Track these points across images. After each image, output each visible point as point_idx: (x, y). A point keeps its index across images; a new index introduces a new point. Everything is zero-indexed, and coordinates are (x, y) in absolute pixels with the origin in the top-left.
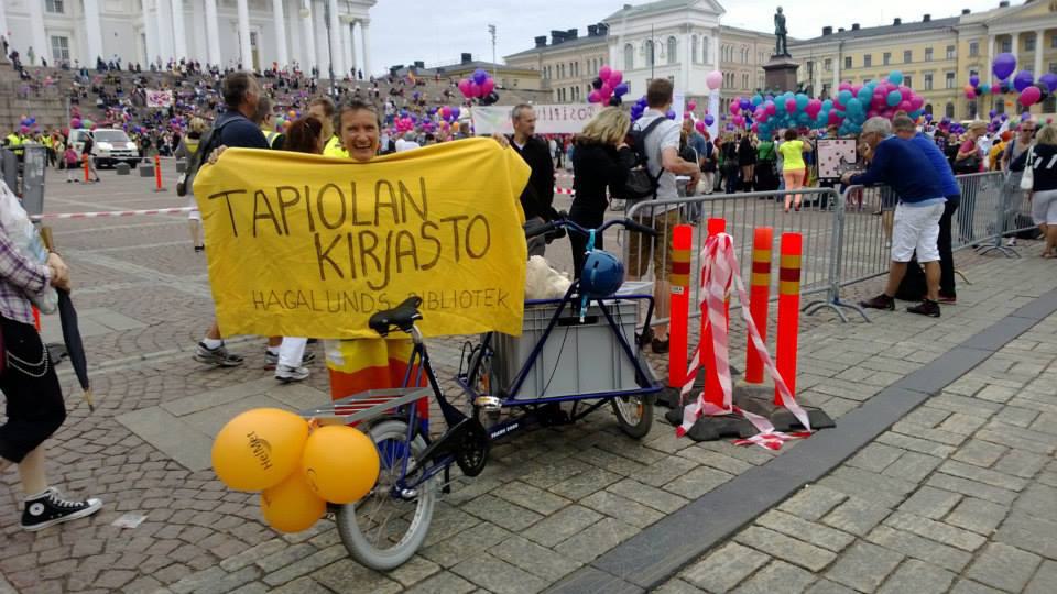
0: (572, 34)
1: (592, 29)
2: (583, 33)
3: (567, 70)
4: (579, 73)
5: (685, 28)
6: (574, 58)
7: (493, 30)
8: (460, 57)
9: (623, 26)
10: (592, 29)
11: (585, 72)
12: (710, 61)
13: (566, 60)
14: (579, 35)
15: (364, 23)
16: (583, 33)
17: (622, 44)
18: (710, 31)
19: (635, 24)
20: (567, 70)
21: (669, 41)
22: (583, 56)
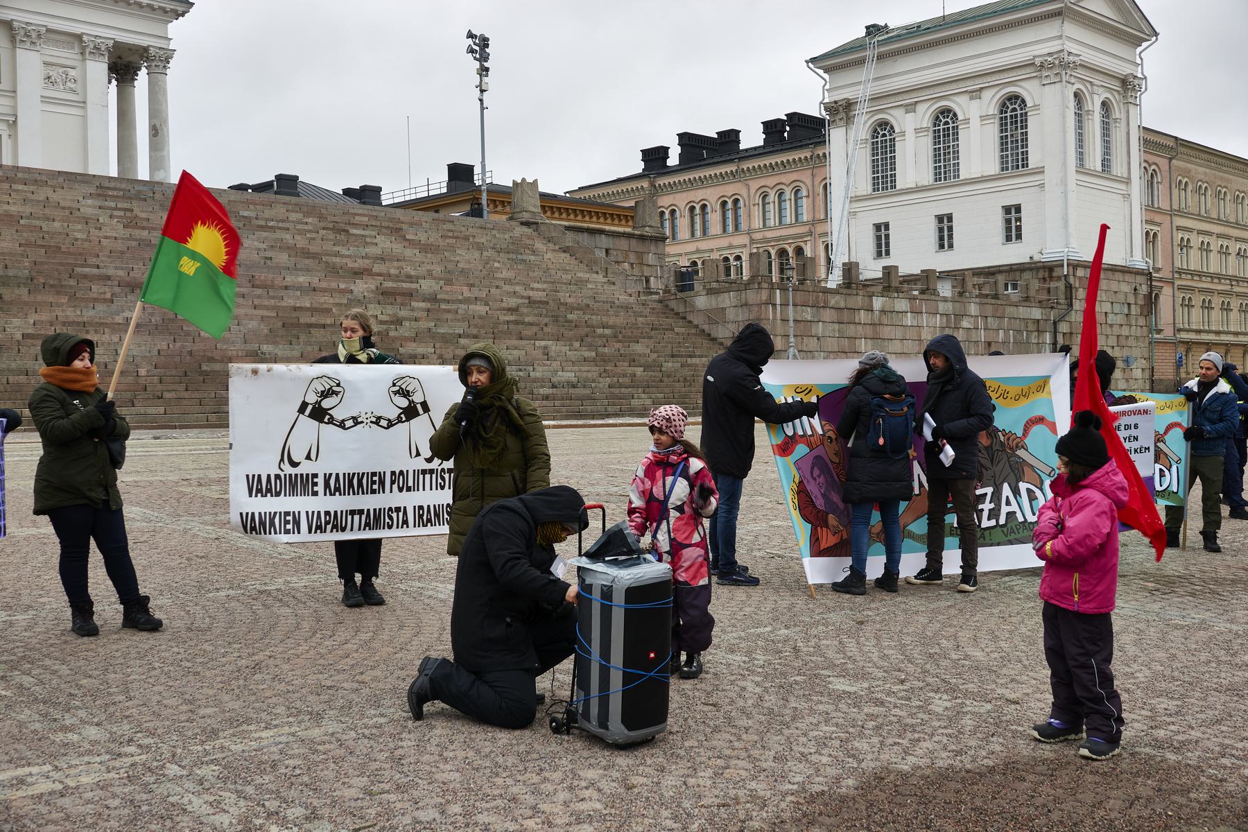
0: (729, 138)
1: (772, 128)
2: (752, 138)
3: (714, 218)
4: (744, 226)
5: (1053, 67)
6: (729, 190)
7: (480, 47)
8: (444, 176)
9: (867, 73)
10: (772, 128)
11: (757, 223)
12: (1118, 169)
13: (711, 195)
14: (742, 147)
15: (158, 60)
16: (752, 138)
17: (862, 126)
18: (1116, 85)
19: (904, 64)
20: (714, 218)
21: (1003, 107)
22: (754, 185)
